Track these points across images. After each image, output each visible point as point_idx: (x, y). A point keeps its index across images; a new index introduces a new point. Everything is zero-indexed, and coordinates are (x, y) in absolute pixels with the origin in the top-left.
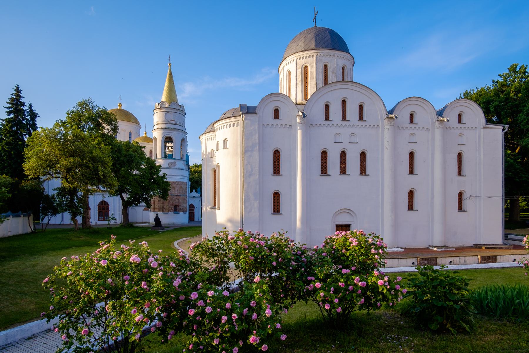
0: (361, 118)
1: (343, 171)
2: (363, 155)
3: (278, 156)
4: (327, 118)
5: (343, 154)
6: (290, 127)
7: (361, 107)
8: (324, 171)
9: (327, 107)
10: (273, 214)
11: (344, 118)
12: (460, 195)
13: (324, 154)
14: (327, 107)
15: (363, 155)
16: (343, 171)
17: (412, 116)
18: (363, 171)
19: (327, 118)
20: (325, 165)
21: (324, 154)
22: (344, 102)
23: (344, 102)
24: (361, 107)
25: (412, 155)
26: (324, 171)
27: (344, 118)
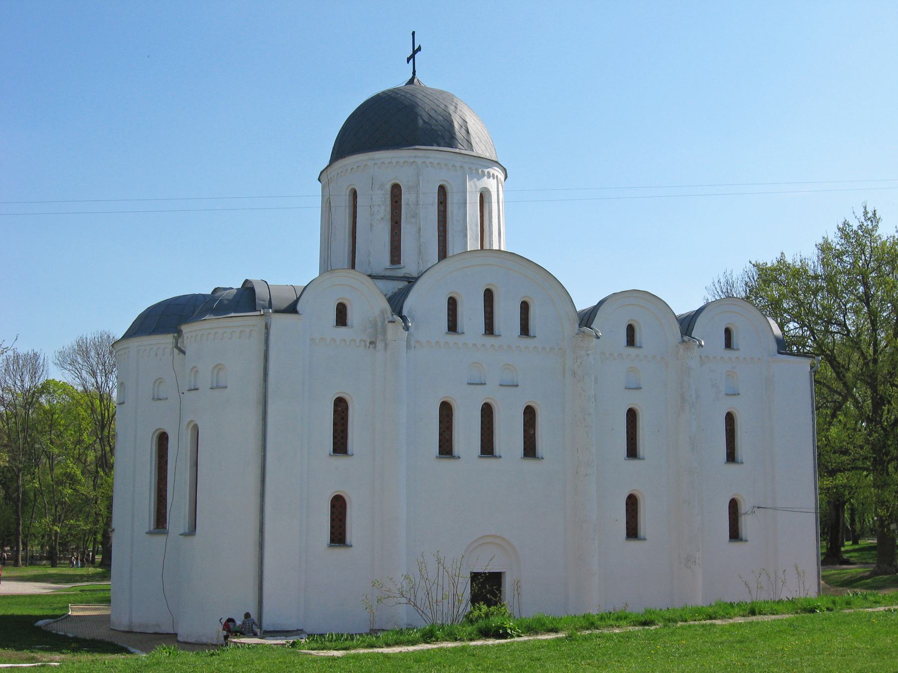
0: (525, 330)
1: (487, 448)
2: (530, 414)
3: (343, 412)
4: (453, 327)
5: (487, 412)
6: (372, 346)
7: (525, 307)
8: (446, 448)
9: (452, 304)
10: (330, 546)
11: (489, 329)
12: (734, 505)
13: (446, 410)
14: (452, 304)
15: (530, 414)
16: (487, 448)
17: (631, 330)
18: (530, 450)
19: (453, 327)
20: (448, 435)
21: (446, 410)
22: (489, 296)
23: (489, 296)
24: (525, 307)
25: (632, 416)
26: (446, 448)
27: (489, 329)
